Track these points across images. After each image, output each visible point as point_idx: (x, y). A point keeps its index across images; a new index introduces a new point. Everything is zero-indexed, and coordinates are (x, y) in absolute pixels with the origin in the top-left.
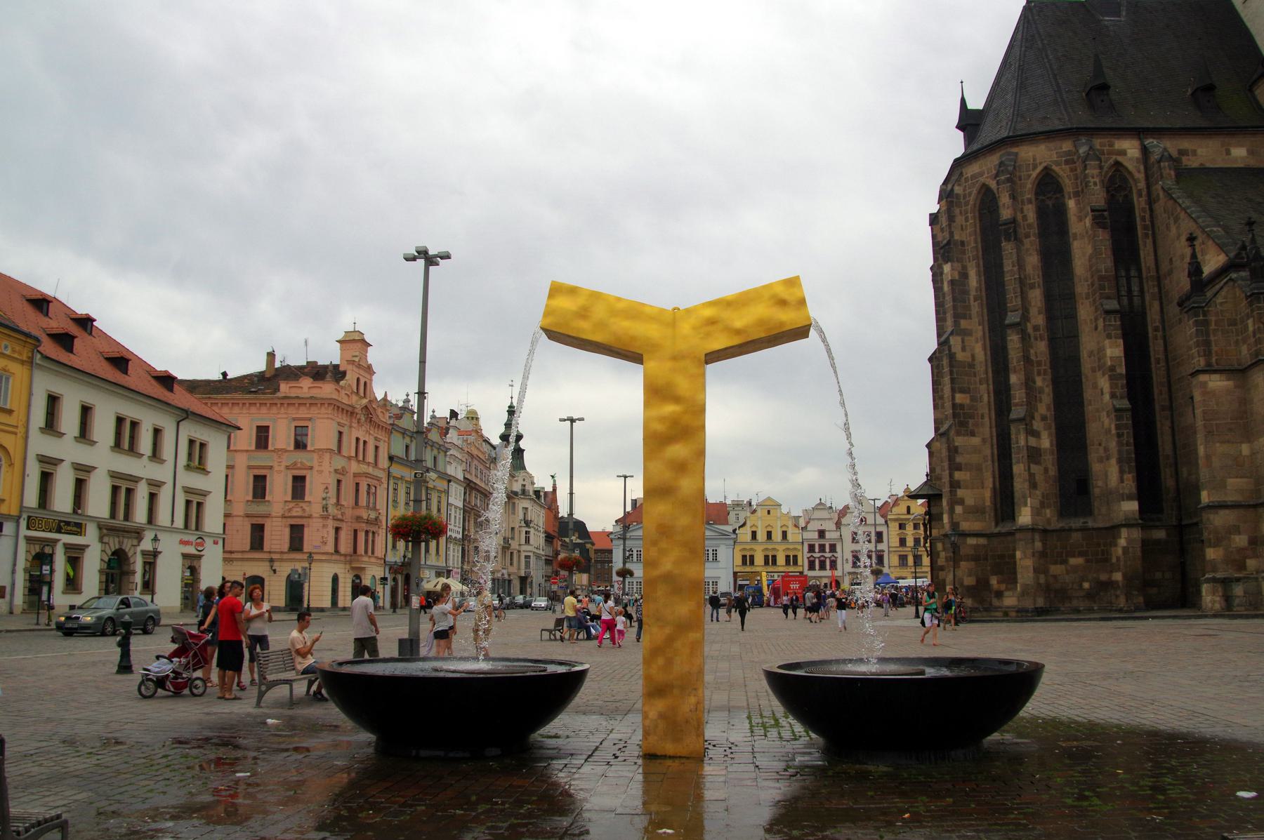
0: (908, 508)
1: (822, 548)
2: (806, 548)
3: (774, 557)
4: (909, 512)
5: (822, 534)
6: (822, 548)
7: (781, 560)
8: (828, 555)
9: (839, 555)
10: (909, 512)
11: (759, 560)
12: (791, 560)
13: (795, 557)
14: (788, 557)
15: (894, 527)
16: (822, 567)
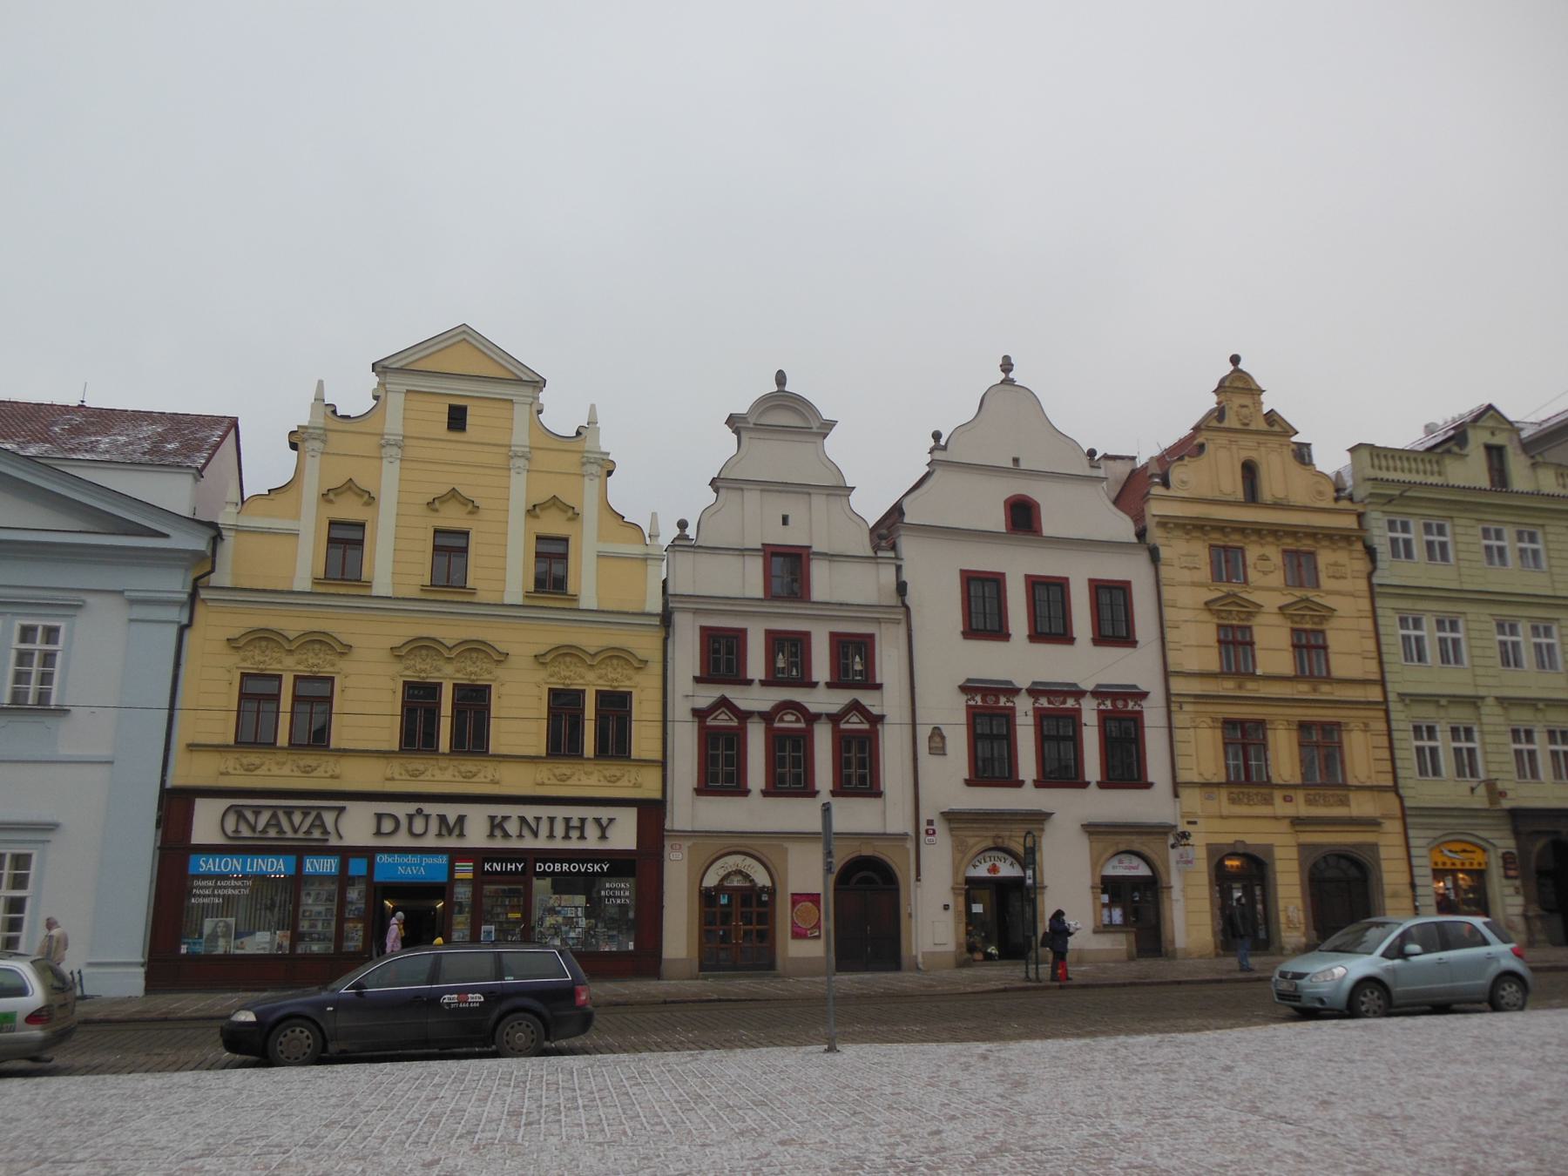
0: (1249, 471)
1: (789, 650)
2: (687, 656)
3: (474, 700)
4: (1252, 494)
5: (789, 568)
6: (789, 650)
7: (519, 721)
8: (824, 700)
9: (889, 702)
10: (1252, 494)
11: (367, 710)
12: (588, 724)
13: (616, 706)
14: (563, 705)
15: (1187, 559)
16: (790, 778)
